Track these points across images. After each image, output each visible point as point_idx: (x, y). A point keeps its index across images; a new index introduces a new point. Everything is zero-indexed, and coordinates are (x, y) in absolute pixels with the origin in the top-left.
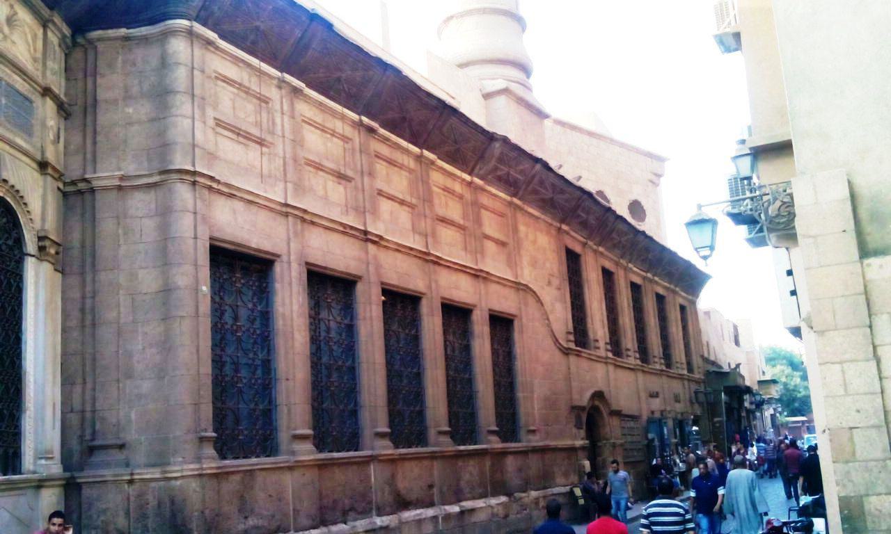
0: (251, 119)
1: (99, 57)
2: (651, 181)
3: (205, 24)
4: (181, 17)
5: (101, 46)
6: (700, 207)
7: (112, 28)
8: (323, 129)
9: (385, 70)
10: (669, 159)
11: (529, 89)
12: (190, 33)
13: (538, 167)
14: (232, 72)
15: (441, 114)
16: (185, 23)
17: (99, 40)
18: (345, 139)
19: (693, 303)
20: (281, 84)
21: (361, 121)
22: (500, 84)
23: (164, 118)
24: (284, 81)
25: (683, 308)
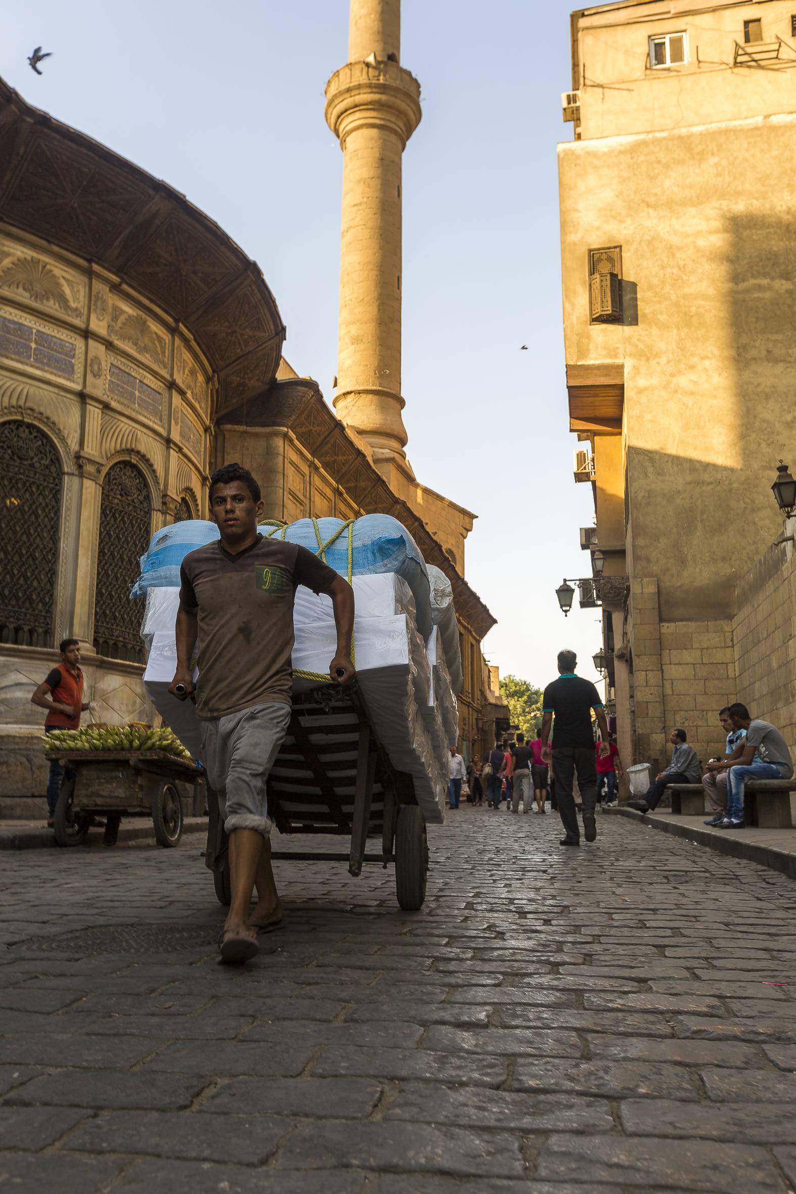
0: (298, 488)
1: (226, 441)
2: (462, 535)
3: (292, 431)
4: (283, 426)
5: (227, 435)
6: (565, 580)
7: (237, 425)
8: (322, 494)
9: (358, 456)
10: (477, 517)
11: (403, 456)
12: (286, 436)
13: (417, 524)
14: (294, 457)
15: (375, 484)
16: (286, 429)
17: (230, 431)
18: (329, 500)
19: (479, 642)
20: (312, 465)
21: (338, 488)
22: (387, 453)
23: (267, 487)
24: (314, 463)
25: (472, 645)
